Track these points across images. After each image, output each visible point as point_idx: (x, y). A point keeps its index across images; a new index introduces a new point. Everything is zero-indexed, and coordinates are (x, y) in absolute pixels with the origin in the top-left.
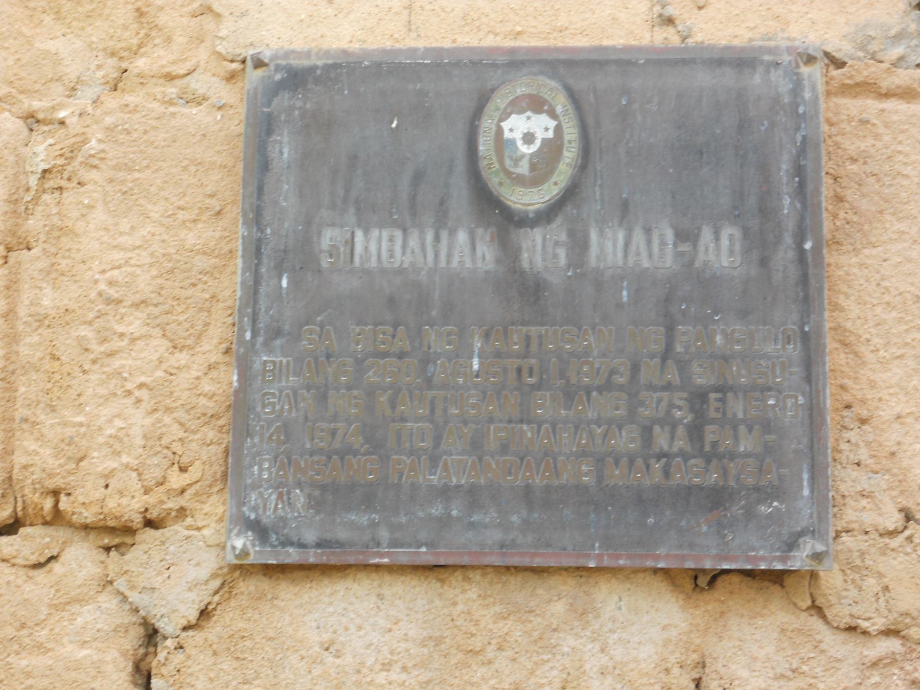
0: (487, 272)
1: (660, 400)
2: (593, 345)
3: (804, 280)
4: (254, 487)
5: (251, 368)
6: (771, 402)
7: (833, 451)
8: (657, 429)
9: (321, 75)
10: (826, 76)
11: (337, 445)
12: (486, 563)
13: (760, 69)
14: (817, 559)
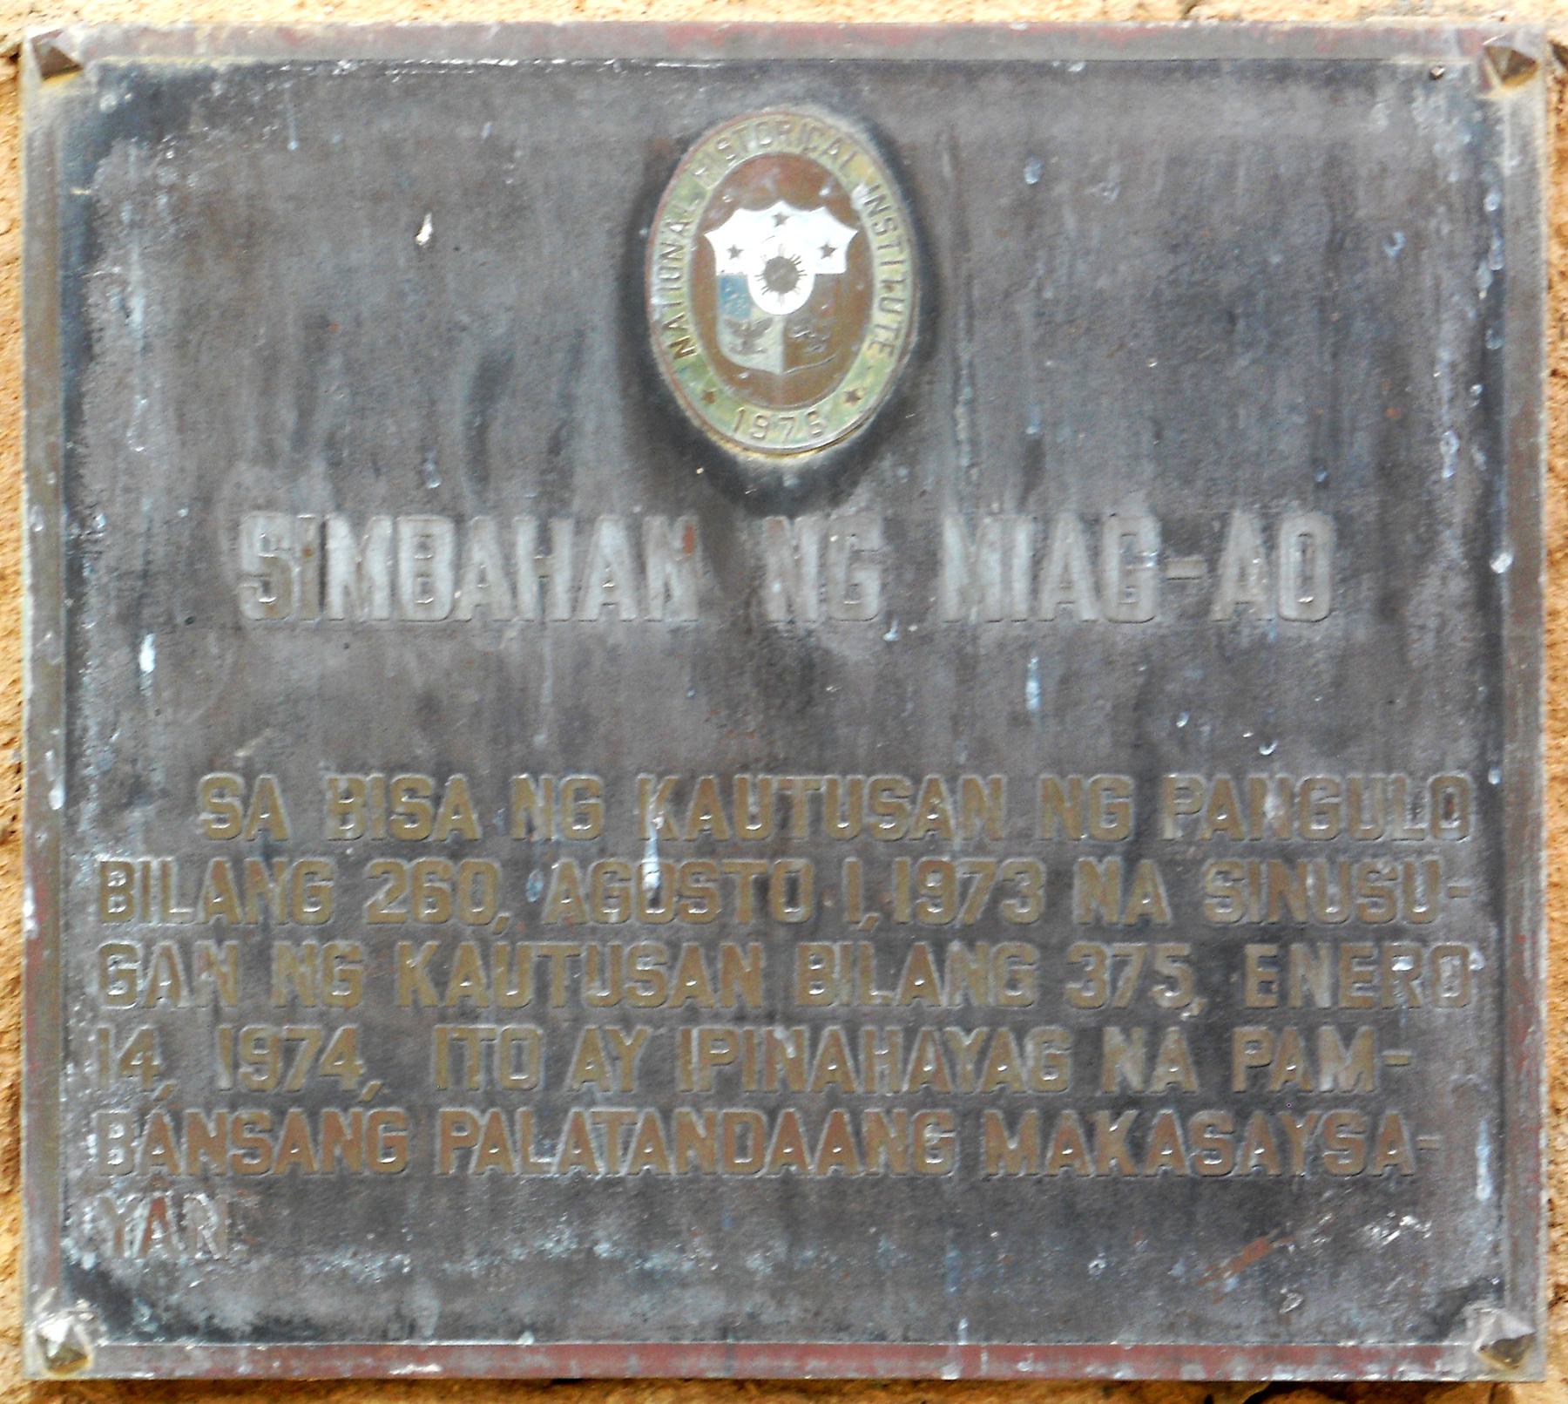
0: (675, 631)
1: (1121, 963)
2: (952, 822)
3: (1490, 653)
4: (91, 1186)
5: (68, 883)
6: (1401, 966)
7: (1552, 1089)
8: (1113, 1036)
9: (224, 97)
10: (1559, 111)
11: (298, 1079)
12: (684, 1373)
13: (1388, 92)
14: (1507, 1355)
